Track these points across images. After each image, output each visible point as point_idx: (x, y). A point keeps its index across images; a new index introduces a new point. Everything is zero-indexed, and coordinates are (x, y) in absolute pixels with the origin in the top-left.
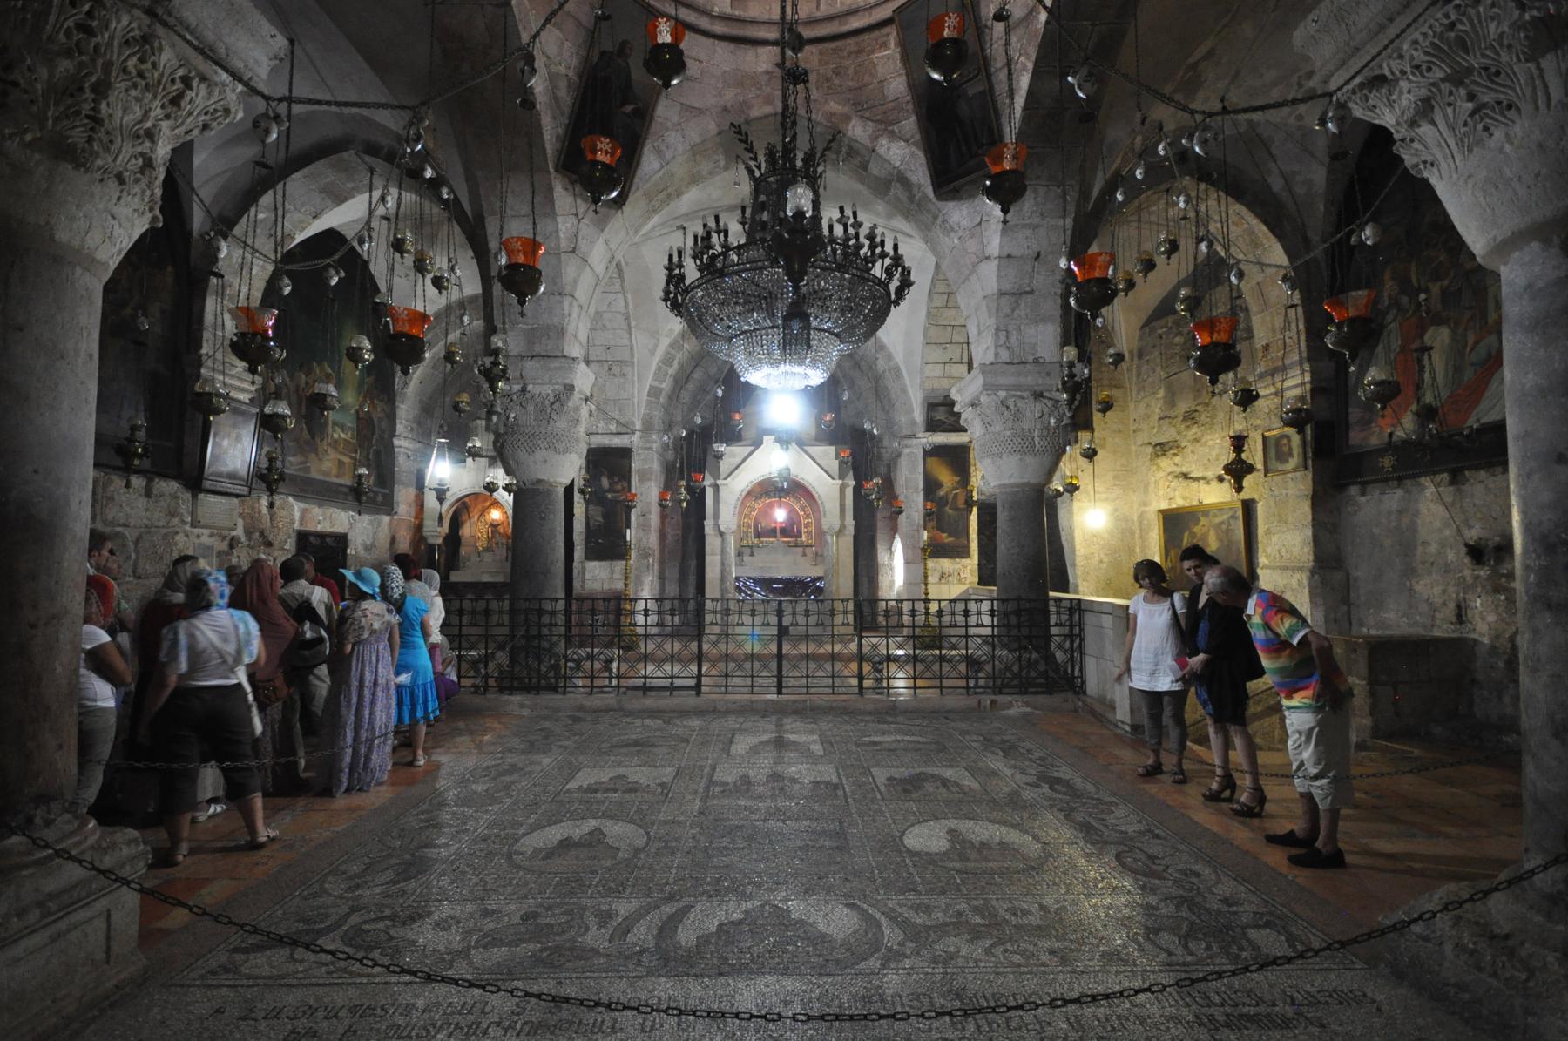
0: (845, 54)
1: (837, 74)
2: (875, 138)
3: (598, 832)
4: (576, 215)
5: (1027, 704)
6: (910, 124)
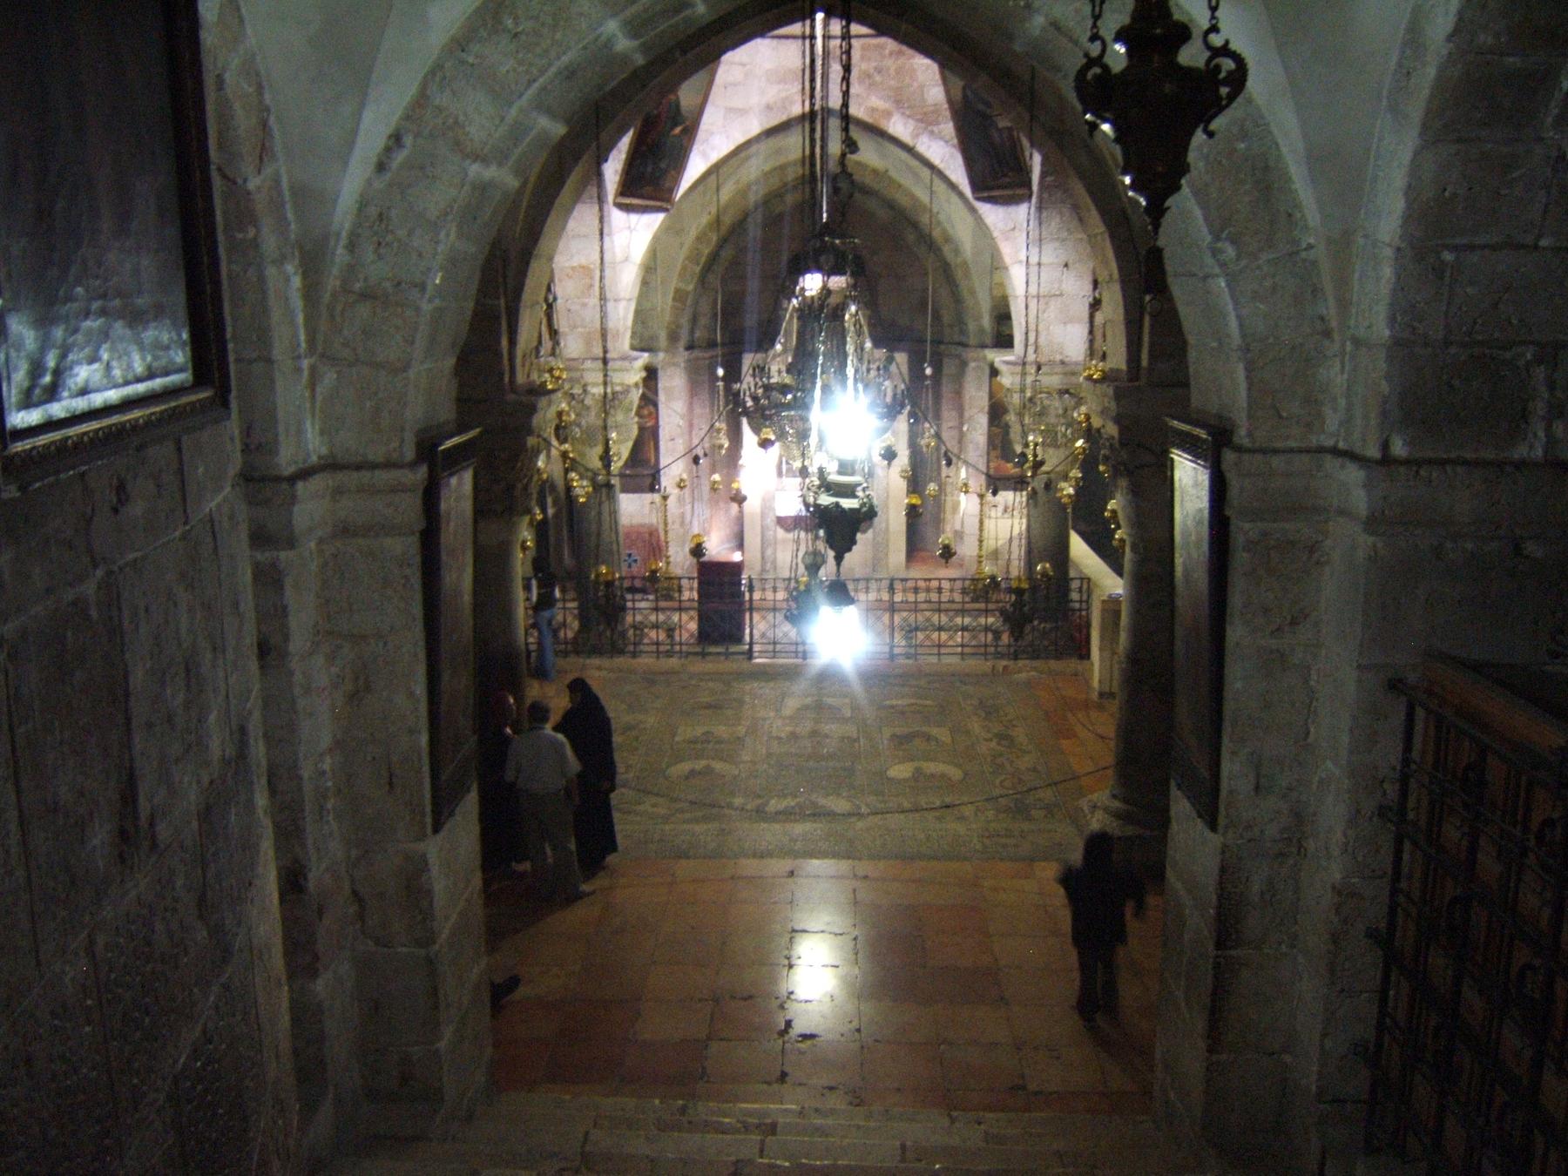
0: (887, 52)
1: (879, 72)
2: (916, 136)
3: (708, 767)
4: (629, 227)
5: (1035, 669)
6: (948, 128)
